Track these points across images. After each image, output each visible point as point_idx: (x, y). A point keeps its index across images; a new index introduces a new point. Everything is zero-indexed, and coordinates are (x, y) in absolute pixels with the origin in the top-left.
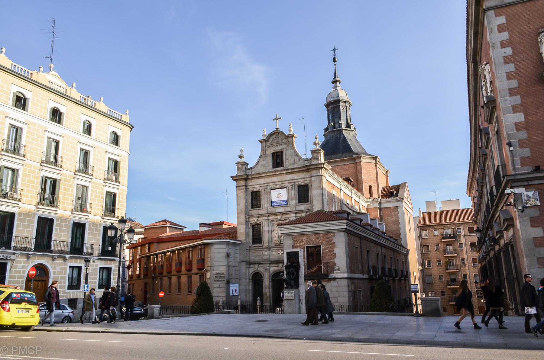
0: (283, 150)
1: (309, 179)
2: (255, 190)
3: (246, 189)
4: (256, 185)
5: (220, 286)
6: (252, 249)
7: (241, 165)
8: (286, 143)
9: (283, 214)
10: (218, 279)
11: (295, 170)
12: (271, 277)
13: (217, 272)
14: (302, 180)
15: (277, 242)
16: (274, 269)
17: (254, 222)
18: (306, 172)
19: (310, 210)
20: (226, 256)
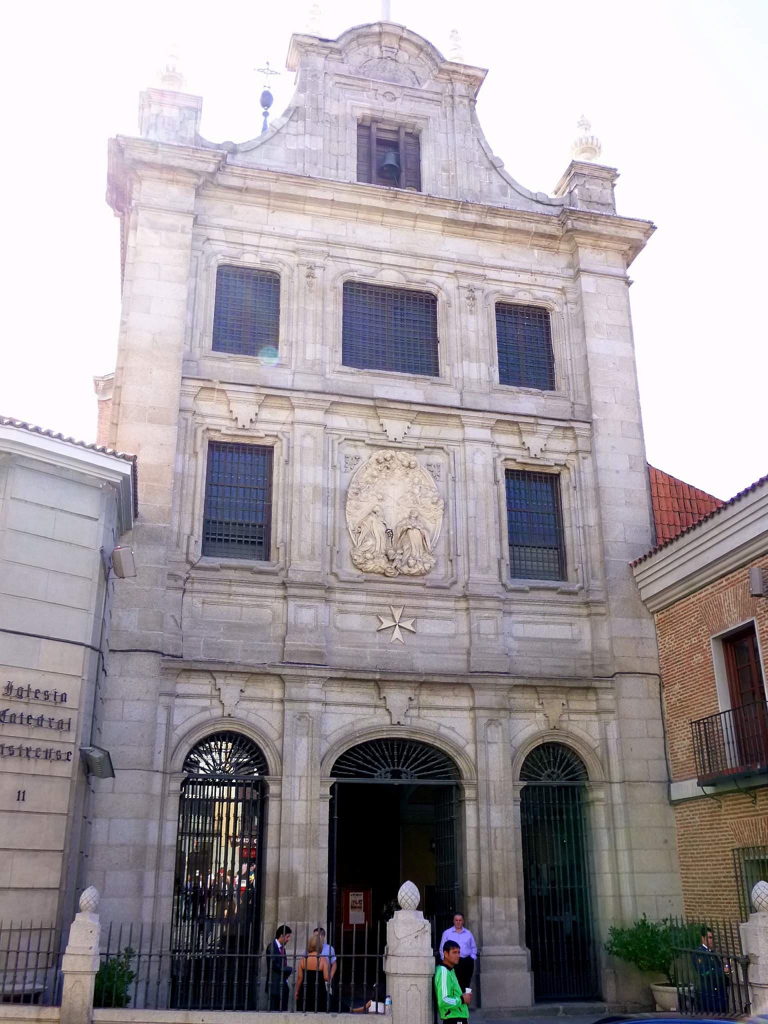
0: (420, 123)
1: (560, 284)
2: (250, 260)
3: (195, 238)
4: (261, 234)
5: (21, 796)
6: (202, 581)
7: (180, 109)
8: (435, 97)
9: (420, 412)
10: (16, 744)
11: (500, 222)
12: (329, 771)
13: (20, 680)
14: (525, 278)
15: (383, 563)
16: (349, 719)
17: (228, 423)
18: (545, 247)
19: (573, 424)
20: (96, 579)
